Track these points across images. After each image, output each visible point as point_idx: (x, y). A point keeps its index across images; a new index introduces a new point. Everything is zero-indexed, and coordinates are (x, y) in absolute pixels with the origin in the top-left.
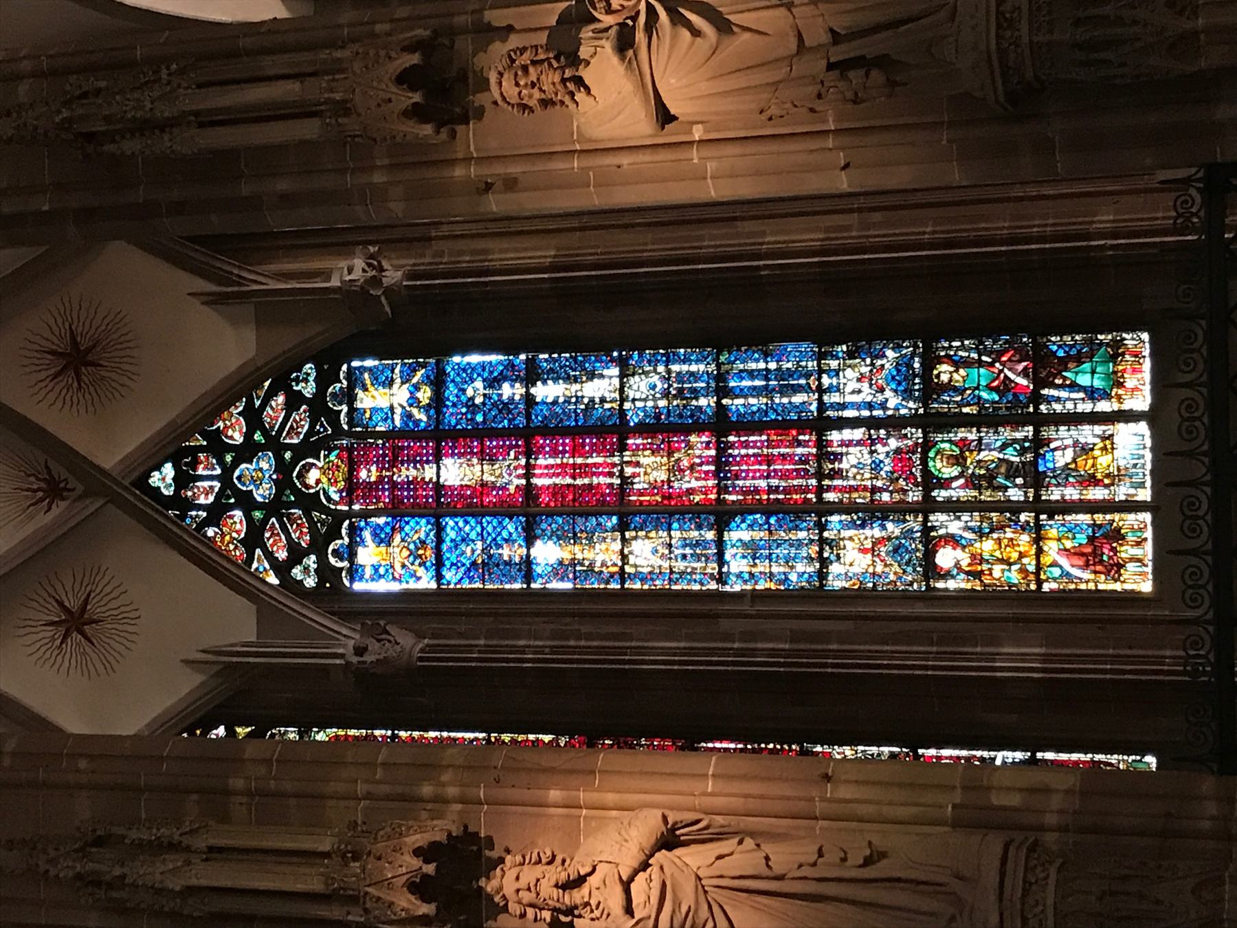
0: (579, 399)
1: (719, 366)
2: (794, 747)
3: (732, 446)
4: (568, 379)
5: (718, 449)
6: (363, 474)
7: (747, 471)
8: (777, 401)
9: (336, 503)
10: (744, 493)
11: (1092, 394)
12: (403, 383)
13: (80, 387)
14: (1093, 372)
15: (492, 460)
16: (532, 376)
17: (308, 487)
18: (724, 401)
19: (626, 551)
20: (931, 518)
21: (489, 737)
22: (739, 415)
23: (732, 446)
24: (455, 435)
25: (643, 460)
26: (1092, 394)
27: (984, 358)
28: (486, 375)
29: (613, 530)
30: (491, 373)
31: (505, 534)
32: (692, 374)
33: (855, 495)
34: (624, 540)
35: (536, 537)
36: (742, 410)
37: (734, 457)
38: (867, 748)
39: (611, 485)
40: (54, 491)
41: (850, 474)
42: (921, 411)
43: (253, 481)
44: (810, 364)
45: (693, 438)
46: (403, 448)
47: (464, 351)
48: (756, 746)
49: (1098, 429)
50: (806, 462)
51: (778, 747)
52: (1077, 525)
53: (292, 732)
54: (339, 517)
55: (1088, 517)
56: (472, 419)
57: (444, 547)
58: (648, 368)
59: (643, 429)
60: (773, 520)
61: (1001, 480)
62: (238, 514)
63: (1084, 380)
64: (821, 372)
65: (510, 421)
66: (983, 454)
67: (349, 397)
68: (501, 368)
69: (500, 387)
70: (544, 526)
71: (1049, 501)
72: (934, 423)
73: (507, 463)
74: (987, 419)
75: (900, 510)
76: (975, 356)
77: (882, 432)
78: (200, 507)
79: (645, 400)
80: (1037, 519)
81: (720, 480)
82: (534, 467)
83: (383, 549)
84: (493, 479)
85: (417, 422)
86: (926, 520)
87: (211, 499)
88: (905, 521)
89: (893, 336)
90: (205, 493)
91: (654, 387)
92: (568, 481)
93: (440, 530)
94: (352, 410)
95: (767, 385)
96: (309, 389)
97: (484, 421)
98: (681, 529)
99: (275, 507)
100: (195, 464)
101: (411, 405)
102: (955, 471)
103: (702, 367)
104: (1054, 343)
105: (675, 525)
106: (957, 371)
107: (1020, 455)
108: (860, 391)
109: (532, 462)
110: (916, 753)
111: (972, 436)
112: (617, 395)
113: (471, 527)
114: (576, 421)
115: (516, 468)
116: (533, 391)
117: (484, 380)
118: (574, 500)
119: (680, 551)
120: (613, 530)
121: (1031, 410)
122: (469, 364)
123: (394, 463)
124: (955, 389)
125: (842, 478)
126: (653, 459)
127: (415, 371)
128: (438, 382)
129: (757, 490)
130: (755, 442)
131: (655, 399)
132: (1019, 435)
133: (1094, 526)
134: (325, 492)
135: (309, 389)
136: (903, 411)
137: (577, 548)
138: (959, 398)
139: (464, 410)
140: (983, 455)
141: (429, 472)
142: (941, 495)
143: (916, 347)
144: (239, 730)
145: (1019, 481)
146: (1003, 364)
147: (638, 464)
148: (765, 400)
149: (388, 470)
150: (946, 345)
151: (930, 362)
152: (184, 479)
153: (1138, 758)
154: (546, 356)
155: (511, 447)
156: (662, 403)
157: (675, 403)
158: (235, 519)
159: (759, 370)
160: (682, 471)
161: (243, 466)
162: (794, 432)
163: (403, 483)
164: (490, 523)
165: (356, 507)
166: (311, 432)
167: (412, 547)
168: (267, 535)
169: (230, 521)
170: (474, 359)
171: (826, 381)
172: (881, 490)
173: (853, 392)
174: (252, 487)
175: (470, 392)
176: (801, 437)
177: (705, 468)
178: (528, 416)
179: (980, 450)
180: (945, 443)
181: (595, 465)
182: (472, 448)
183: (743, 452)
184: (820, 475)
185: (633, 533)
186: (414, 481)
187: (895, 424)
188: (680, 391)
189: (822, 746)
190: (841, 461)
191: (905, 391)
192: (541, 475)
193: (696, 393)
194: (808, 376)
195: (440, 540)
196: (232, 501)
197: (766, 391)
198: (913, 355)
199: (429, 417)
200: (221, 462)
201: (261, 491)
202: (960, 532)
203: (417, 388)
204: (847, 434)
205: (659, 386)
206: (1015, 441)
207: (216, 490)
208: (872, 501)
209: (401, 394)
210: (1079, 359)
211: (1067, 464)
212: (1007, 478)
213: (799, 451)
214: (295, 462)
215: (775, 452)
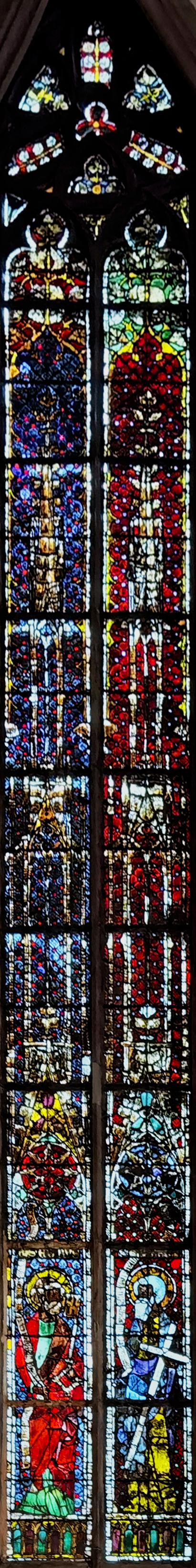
2: (185, 1076)
21: (184, 617)
38: (188, 1180)
48: (185, 1021)
51: (185, 1054)
53: (184, 292)
110: (184, 1246)
144: (184, 203)
153: (189, 1539)
189: (188, 1116)
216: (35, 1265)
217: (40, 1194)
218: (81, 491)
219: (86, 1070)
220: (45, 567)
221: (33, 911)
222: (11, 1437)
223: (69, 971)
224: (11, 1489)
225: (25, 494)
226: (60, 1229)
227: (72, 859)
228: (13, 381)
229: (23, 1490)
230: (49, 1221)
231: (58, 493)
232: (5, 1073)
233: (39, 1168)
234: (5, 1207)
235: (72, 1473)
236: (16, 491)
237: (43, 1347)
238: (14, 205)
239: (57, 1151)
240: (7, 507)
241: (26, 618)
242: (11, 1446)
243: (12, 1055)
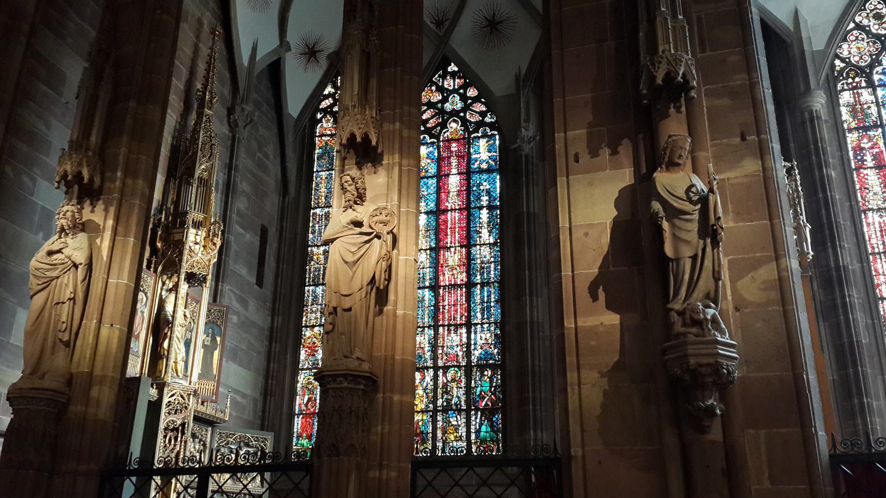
0: (481, 228)
1: (493, 282)
3: (461, 290)
4: (489, 222)
5: (460, 285)
6: (454, 145)
7: (451, 297)
8: (479, 307)
9: (443, 136)
10: (443, 296)
11: (478, 432)
12: (489, 157)
13: (482, 28)
14: (486, 432)
15: (458, 195)
16: (490, 208)
17: (450, 124)
18: (479, 286)
19: (422, 251)
20: (432, 370)
22: (473, 292)
23: (461, 290)
24: (468, 179)
25: (456, 255)
26: (478, 432)
27: (493, 389)
28: (492, 189)
30: (492, 192)
31: (429, 203)
32: (490, 272)
33: (441, 339)
34: (426, 250)
35: (428, 216)
36: (475, 293)
37: (457, 291)
39: (447, 243)
40: (439, 24)
41: (449, 337)
42: (473, 364)
43: (453, 102)
44: (493, 319)
45: (464, 274)
46: (464, 159)
47: (501, 180)
49: (464, 434)
50: (454, 320)
52: (428, 427)
54: (437, 137)
55: (431, 431)
56: (474, 186)
57: (425, 180)
58: (492, 255)
59: (469, 253)
60: (432, 308)
61: (445, 396)
62: (440, 98)
63: (484, 428)
64: (490, 324)
65: (473, 201)
66: (456, 389)
67: (484, 136)
68: (494, 195)
69: (486, 196)
70: (432, 218)
71: (437, 415)
72: (468, 370)
73: (457, 201)
74: (469, 390)
75: (435, 358)
76: (494, 384)
77: (465, 349)
78: (443, 82)
79: (480, 254)
80: (430, 411)
81: (448, 286)
82: (455, 212)
83: (426, 156)
84: (451, 196)
85: (474, 164)
86: (430, 368)
87: (446, 86)
88: (431, 359)
89: (502, 353)
90: (449, 83)
91: (485, 257)
92: (449, 226)
93: (432, 177)
94: (479, 138)
95: (484, 302)
96: (488, 119)
97: (473, 191)
98: (430, 272)
99: (442, 112)
100: (460, 78)
101: (480, 161)
102: (449, 379)
103: (492, 276)
104: (498, 416)
105: (431, 270)
106: (488, 378)
107: (455, 404)
108: (481, 339)
109: (457, 211)
111: (463, 385)
112: (482, 243)
113: (433, 189)
114: (473, 227)
115: (455, 205)
116: (485, 209)
117: (489, 189)
118: (442, 229)
119: (421, 272)
120: (430, 245)
121: (473, 408)
122: (496, 182)
123: (458, 157)
124: (481, 377)
125: (448, 334)
126: (457, 259)
127: (494, 161)
128: (489, 171)
129: (444, 301)
130: (462, 299)
131: (480, 258)
132: (463, 403)
133: (428, 433)
134: (447, 131)
135: (488, 119)
136: (473, 357)
137: (424, 232)
138: (477, 379)
139: (478, 182)
140: (455, 389)
141: (454, 171)
142: (440, 373)
143: (498, 361)
145: (445, 404)
146: (491, 396)
147: (455, 253)
148: (479, 302)
149: (455, 154)
150: (499, 373)
151: (493, 367)
152: (453, 75)
154: (498, 213)
155: (463, 202)
156: (479, 261)
157: (479, 266)
158: (438, 97)
159: (491, 299)
160: (452, 270)
161: (458, 97)
162: (466, 314)
163: (450, 161)
164: (433, 197)
165: (441, 144)
166: (471, 123)
167: (426, 167)
168: (432, 110)
169: (437, 95)
170: (498, 184)
171: (486, 326)
172: (443, 349)
173: (481, 337)
174: (450, 101)
175: (485, 184)
176: (464, 317)
177: (453, 280)
178: (475, 208)
179: (457, 388)
180: (461, 374)
181: (455, 237)
182: (463, 187)
183: (459, 295)
184: (449, 325)
185: (429, 253)
186: (451, 165)
187: (468, 354)
188: (483, 268)
190: (454, 333)
191: (481, 357)
192: (451, 215)
193: (482, 274)
194: (488, 318)
195: (428, 178)
196: (445, 95)
197: (482, 302)
198: (495, 360)
199: (476, 168)
200: (461, 87)
201: (449, 105)
202: (426, 381)
203: (487, 163)
204: (465, 335)
205: (485, 259)
206: (460, 402)
207: (450, 88)
208: (439, 346)
209: (484, 155)
210: (492, 426)
211: (451, 422)
212: (446, 399)
213: (459, 316)
214: (460, 118)
215: (459, 307)
216: (306, 375)
217: (309, 355)
218: (332, 177)
219: (323, 321)
220: (322, 196)
221: (313, 281)
222: (296, 424)
223: (321, 295)
224: (295, 439)
225: (319, 179)
226: (314, 364)
227: (324, 267)
228: (318, 153)
229: (298, 440)
230: (310, 363)
231: (326, 178)
232: (302, 323)
233: (309, 348)
234: (299, 359)
235: (311, 434)
236: (316, 179)
237: (306, 398)
238: (321, 114)
239: (314, 343)
240: (314, 183)
241: (316, 208)
242: (295, 427)
243: (304, 319)
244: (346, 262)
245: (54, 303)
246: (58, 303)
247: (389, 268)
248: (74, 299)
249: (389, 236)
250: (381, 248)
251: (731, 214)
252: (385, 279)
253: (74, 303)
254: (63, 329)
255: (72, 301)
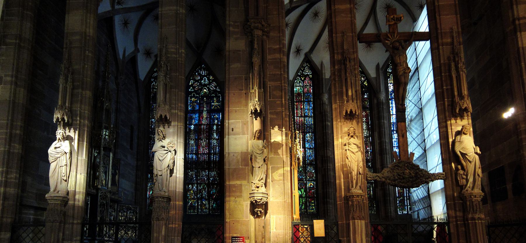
3: (206, 156)
23: (206, 156)
29: (195, 138)
59: (209, 142)
131: (213, 144)
147: (204, 141)
188: (214, 148)
193: (214, 151)
244: (160, 160)
245: (59, 166)
246: (61, 166)
247: (174, 162)
248: (66, 165)
249: (173, 151)
250: (171, 156)
251: (273, 153)
252: (172, 166)
253: (67, 166)
254: (64, 176)
255: (66, 166)
